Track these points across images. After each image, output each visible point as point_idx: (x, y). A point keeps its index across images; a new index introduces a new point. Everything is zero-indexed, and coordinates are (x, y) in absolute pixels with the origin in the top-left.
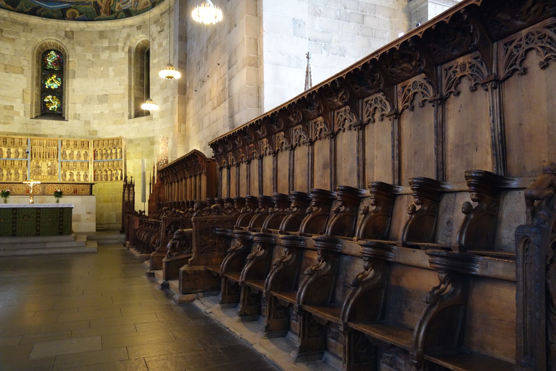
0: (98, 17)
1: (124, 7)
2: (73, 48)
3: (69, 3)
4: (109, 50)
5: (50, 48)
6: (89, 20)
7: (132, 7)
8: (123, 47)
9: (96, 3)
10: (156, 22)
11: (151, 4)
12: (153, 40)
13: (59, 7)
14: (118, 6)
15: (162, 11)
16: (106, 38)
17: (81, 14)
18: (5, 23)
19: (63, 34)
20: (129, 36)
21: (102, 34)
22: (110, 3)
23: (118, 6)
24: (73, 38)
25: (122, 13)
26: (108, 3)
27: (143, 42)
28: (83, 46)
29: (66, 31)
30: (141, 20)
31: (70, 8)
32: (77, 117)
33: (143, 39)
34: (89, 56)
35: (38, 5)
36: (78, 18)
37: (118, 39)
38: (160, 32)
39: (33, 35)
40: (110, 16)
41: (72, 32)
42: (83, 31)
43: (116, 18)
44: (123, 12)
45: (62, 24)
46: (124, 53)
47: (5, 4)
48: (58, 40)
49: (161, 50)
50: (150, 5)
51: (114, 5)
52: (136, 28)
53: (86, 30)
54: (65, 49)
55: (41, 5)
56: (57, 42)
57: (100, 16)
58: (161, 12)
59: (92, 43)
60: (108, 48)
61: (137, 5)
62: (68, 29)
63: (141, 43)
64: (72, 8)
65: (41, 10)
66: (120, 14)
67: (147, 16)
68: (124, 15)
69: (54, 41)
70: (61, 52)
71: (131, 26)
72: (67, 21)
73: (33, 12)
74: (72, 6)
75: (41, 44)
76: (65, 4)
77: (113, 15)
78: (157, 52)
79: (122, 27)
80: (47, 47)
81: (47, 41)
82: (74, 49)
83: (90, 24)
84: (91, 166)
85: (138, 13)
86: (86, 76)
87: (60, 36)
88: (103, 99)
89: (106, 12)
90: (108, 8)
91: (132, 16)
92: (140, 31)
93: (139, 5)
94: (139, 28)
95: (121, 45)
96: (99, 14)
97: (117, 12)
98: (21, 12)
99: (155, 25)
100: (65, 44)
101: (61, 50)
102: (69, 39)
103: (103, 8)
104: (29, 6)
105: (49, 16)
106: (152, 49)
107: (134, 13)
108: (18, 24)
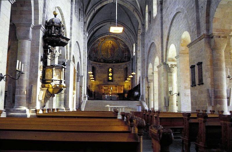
9: (118, 60)
14: (122, 60)
19: (112, 66)
20: (124, 66)
21: (119, 66)
32: (115, 81)
34: (117, 70)
41: (114, 65)
60: (120, 68)
67: (127, 63)
73: (107, 63)
77: (121, 62)
83: (117, 64)
84: (118, 90)
86: (116, 73)
88: (119, 78)
100: (113, 67)
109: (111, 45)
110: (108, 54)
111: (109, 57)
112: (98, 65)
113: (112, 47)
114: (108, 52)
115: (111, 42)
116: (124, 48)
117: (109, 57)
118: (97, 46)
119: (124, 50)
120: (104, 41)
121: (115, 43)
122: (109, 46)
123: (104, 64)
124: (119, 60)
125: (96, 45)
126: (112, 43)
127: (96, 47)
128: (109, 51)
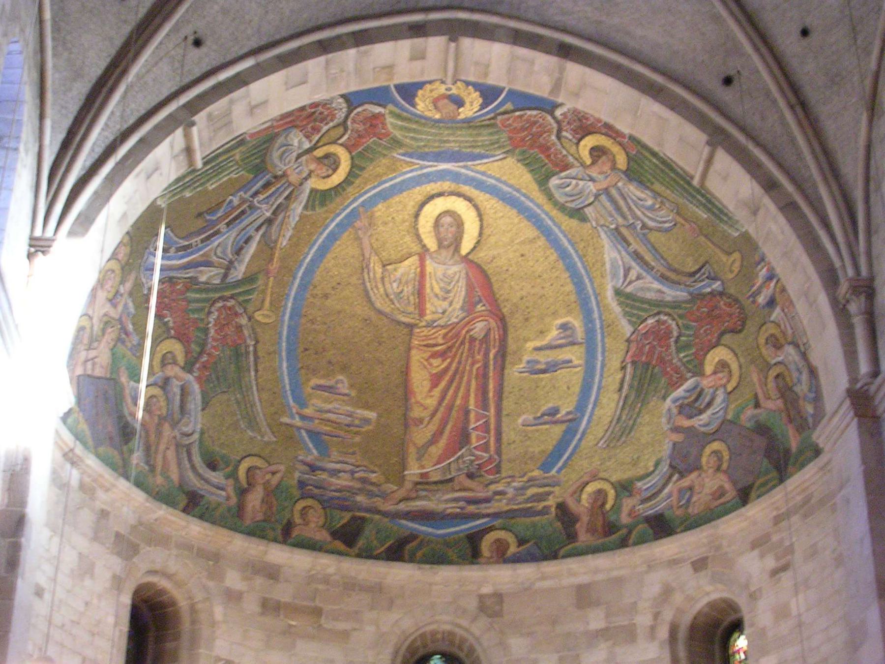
0: (570, 546)
1: (649, 509)
2: (501, 643)
3: (488, 515)
4: (607, 640)
5: (431, 648)
6: (546, 558)
7: (672, 507)
8: (653, 628)
9: (562, 507)
10: (759, 543)
11: (734, 493)
12: (753, 597)
13: (461, 531)
15: (777, 509)
16: (597, 603)
17: (521, 542)
18: (328, 590)
19: (472, 604)
20: (667, 592)
22: (603, 505)
23: (629, 507)
24: (498, 614)
25: (642, 527)
26: (599, 503)
27: (712, 605)
28: (529, 634)
29: (481, 597)
30: (705, 541)
31: (491, 529)
33: (715, 596)
35: (407, 533)
36: (514, 555)
37: (635, 603)
38: (775, 572)
39: (394, 616)
40: (607, 539)
41: (499, 597)
42: (526, 589)
43: (623, 543)
44: (646, 525)
45: (471, 573)
46: (656, 644)
47: (329, 538)
48: (459, 621)
49: (785, 627)
50: (731, 493)
51: (617, 507)
52: (690, 566)
53: (538, 585)
54: (477, 647)
55: (415, 529)
56: (457, 630)
57: (577, 542)
58: (775, 513)
59: (554, 623)
60: (603, 634)
61: (689, 500)
62: (486, 590)
63: (706, 610)
64: (497, 529)
65: (414, 544)
66: (634, 533)
68: (651, 531)
69: (447, 627)
70: (462, 655)
71: (673, 563)
72: (485, 566)
74: (498, 522)
75: (412, 638)
76: (478, 519)
78: (770, 634)
79: (644, 568)
80: (425, 646)
81: (429, 628)
82: (503, 645)
83: (549, 567)
85: (692, 523)
87: (464, 611)
89: (592, 530)
90: (600, 518)
91: (676, 533)
92: (703, 573)
93: (694, 499)
94: (699, 565)
95: (643, 620)
96: (572, 537)
97: (626, 526)
98: (367, 554)
99: (756, 552)
101: (462, 650)
102: (490, 616)
103: (585, 519)
104: (388, 537)
105: (437, 559)
106: (752, 625)
107: (682, 523)
108: (360, 590)
109: (456, 269)
110: (406, 423)
111: (413, 471)
112: (233, 580)
113: (469, 306)
114: (407, 391)
115: (459, 224)
116: (659, 306)
117: (413, 471)
118: (239, 272)
119: (660, 335)
120: (354, 200)
121: (530, 232)
122: (433, 286)
123: (327, 564)
124: (583, 505)
125: (228, 238)
126: (466, 246)
127: (224, 285)
128: (420, 379)
